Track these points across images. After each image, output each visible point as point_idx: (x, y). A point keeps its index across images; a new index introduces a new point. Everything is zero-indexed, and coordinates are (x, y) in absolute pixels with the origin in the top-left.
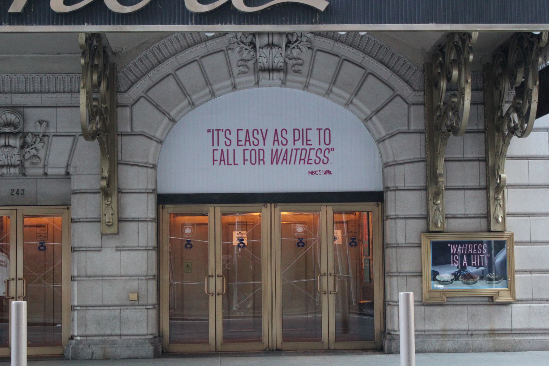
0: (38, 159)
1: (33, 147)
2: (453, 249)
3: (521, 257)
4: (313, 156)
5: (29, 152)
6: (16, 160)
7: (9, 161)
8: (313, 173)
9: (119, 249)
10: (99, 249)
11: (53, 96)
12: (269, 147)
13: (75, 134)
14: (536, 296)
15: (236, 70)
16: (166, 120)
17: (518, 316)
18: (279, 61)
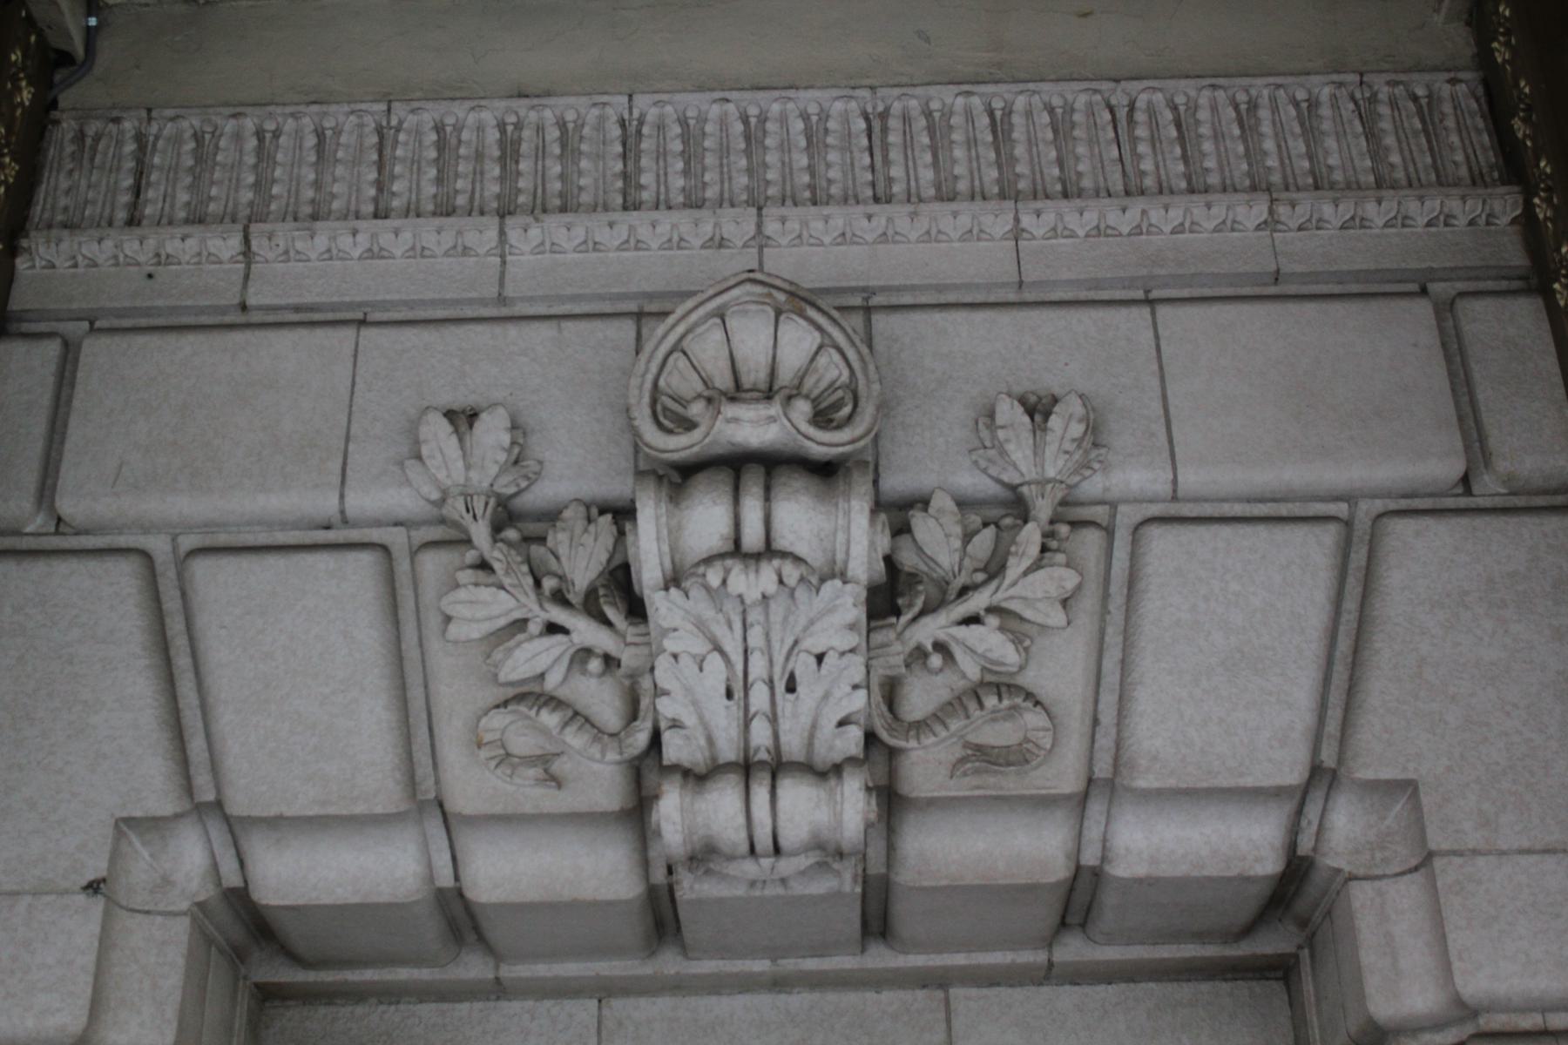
0: (1033, 719)
1: (977, 602)
5: (940, 647)
6: (829, 708)
7: (761, 734)
11: (1113, 218)
13: (1341, 509)
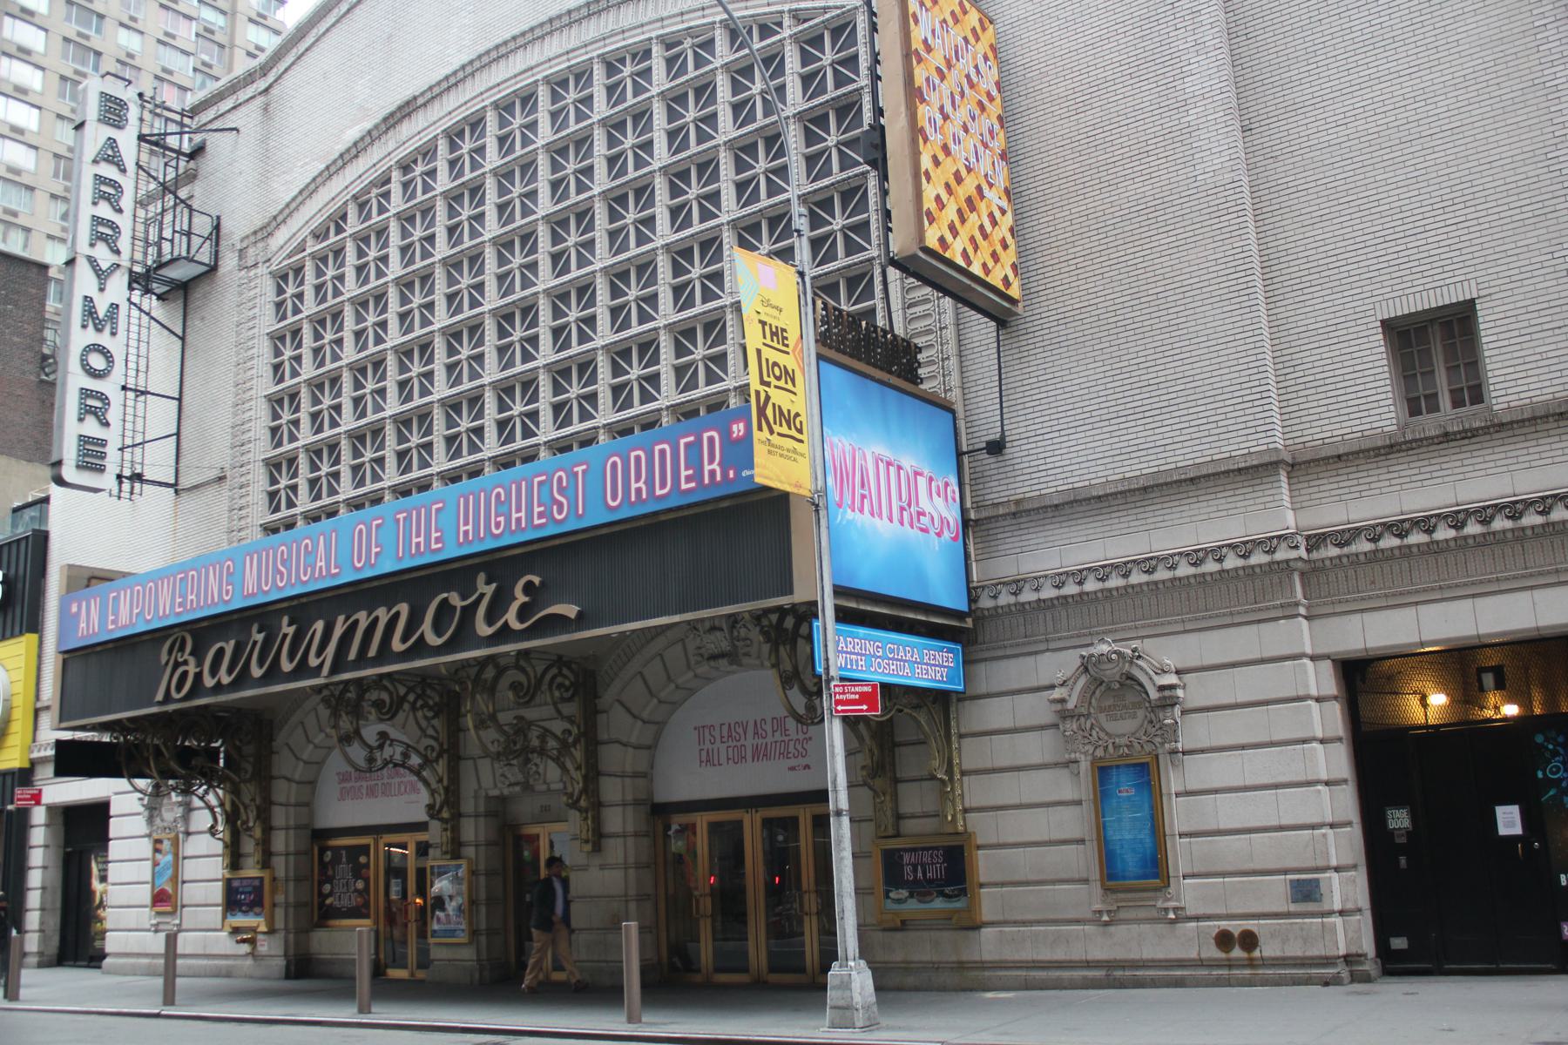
2: (906, 858)
3: (984, 865)
4: (791, 749)
8: (792, 769)
9: (602, 867)
10: (584, 868)
12: (750, 742)
14: (1008, 917)
15: (693, 660)
16: (639, 723)
17: (988, 944)
18: (725, 646)
